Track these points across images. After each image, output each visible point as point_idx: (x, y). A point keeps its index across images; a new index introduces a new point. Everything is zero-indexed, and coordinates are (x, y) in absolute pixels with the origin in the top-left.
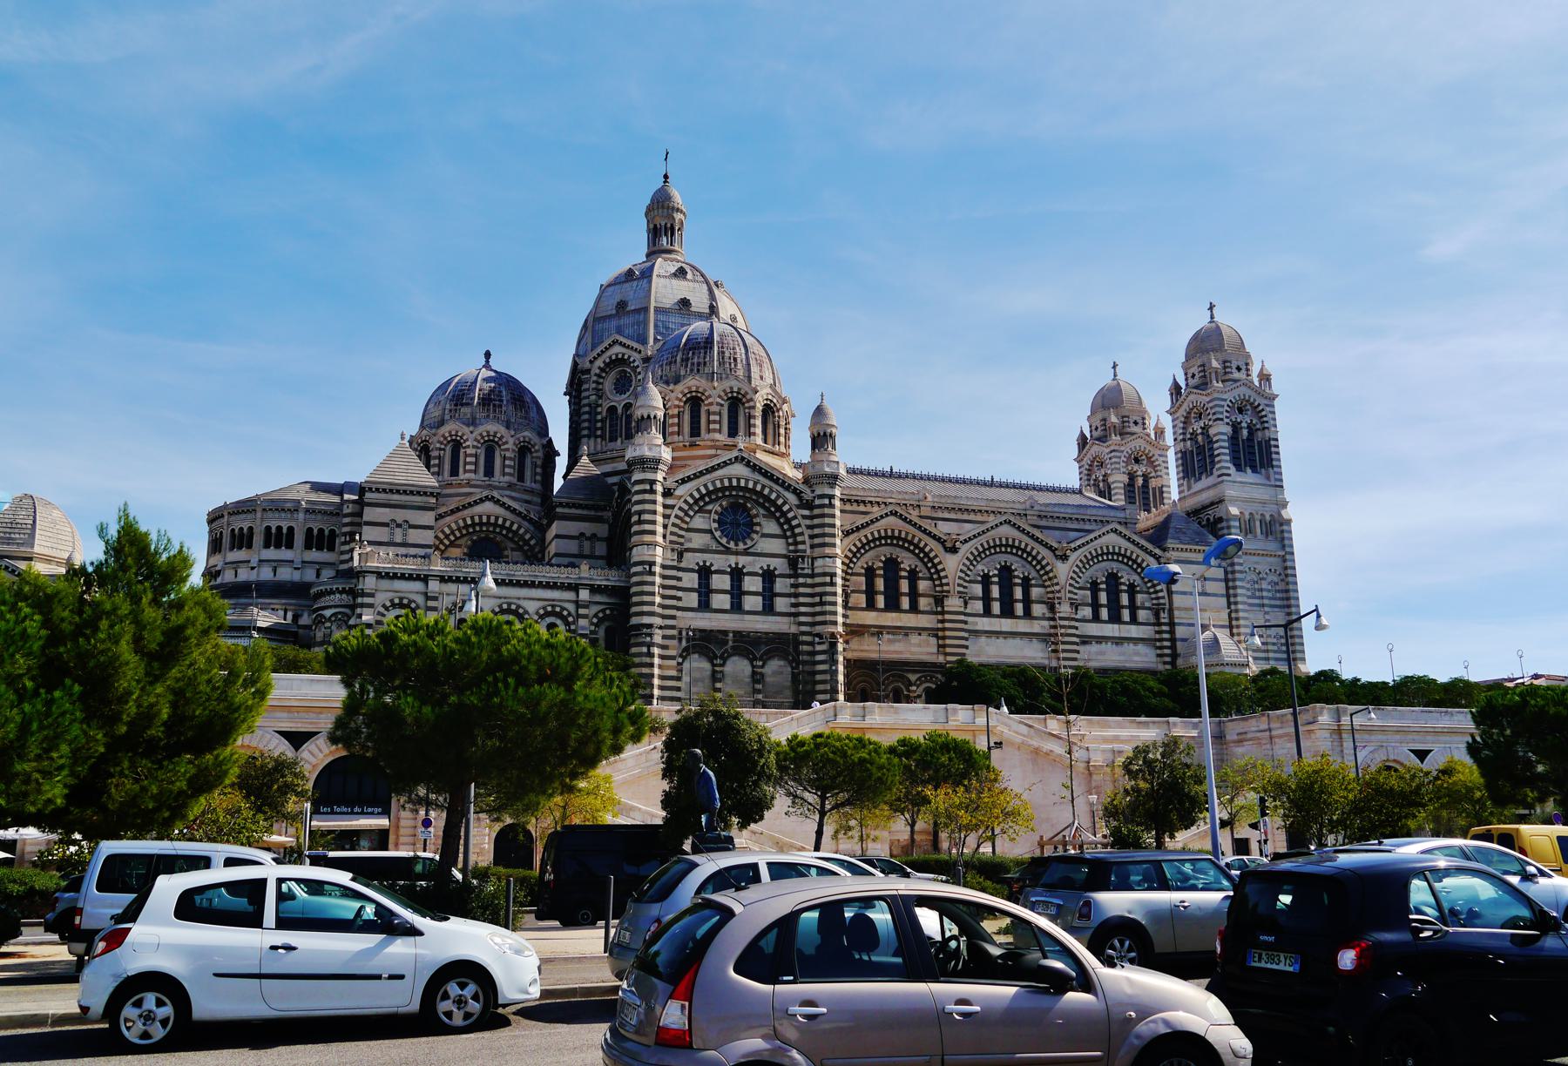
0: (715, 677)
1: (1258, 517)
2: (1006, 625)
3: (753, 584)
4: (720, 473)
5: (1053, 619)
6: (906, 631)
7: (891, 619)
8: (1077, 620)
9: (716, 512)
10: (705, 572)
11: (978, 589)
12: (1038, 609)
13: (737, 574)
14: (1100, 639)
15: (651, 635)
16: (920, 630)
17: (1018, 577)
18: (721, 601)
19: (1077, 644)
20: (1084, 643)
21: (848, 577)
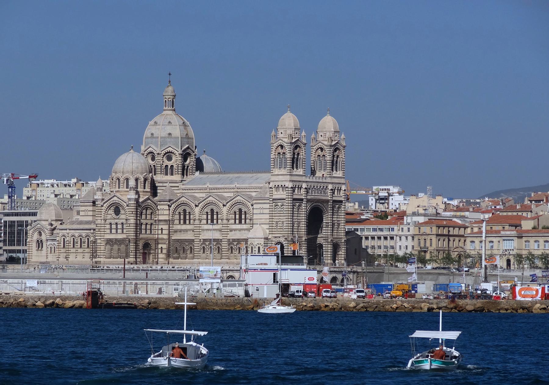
0: (111, 250)
1: (280, 186)
2: (210, 227)
3: (120, 226)
4: (112, 200)
5: (222, 224)
6: (186, 231)
7: (184, 227)
8: (229, 224)
9: (113, 209)
10: (111, 224)
11: (205, 217)
12: (220, 221)
13: (116, 224)
14: (235, 230)
15: (97, 241)
16: (190, 230)
17: (215, 212)
18: (114, 231)
19: (227, 232)
20: (231, 231)
21: (174, 216)
